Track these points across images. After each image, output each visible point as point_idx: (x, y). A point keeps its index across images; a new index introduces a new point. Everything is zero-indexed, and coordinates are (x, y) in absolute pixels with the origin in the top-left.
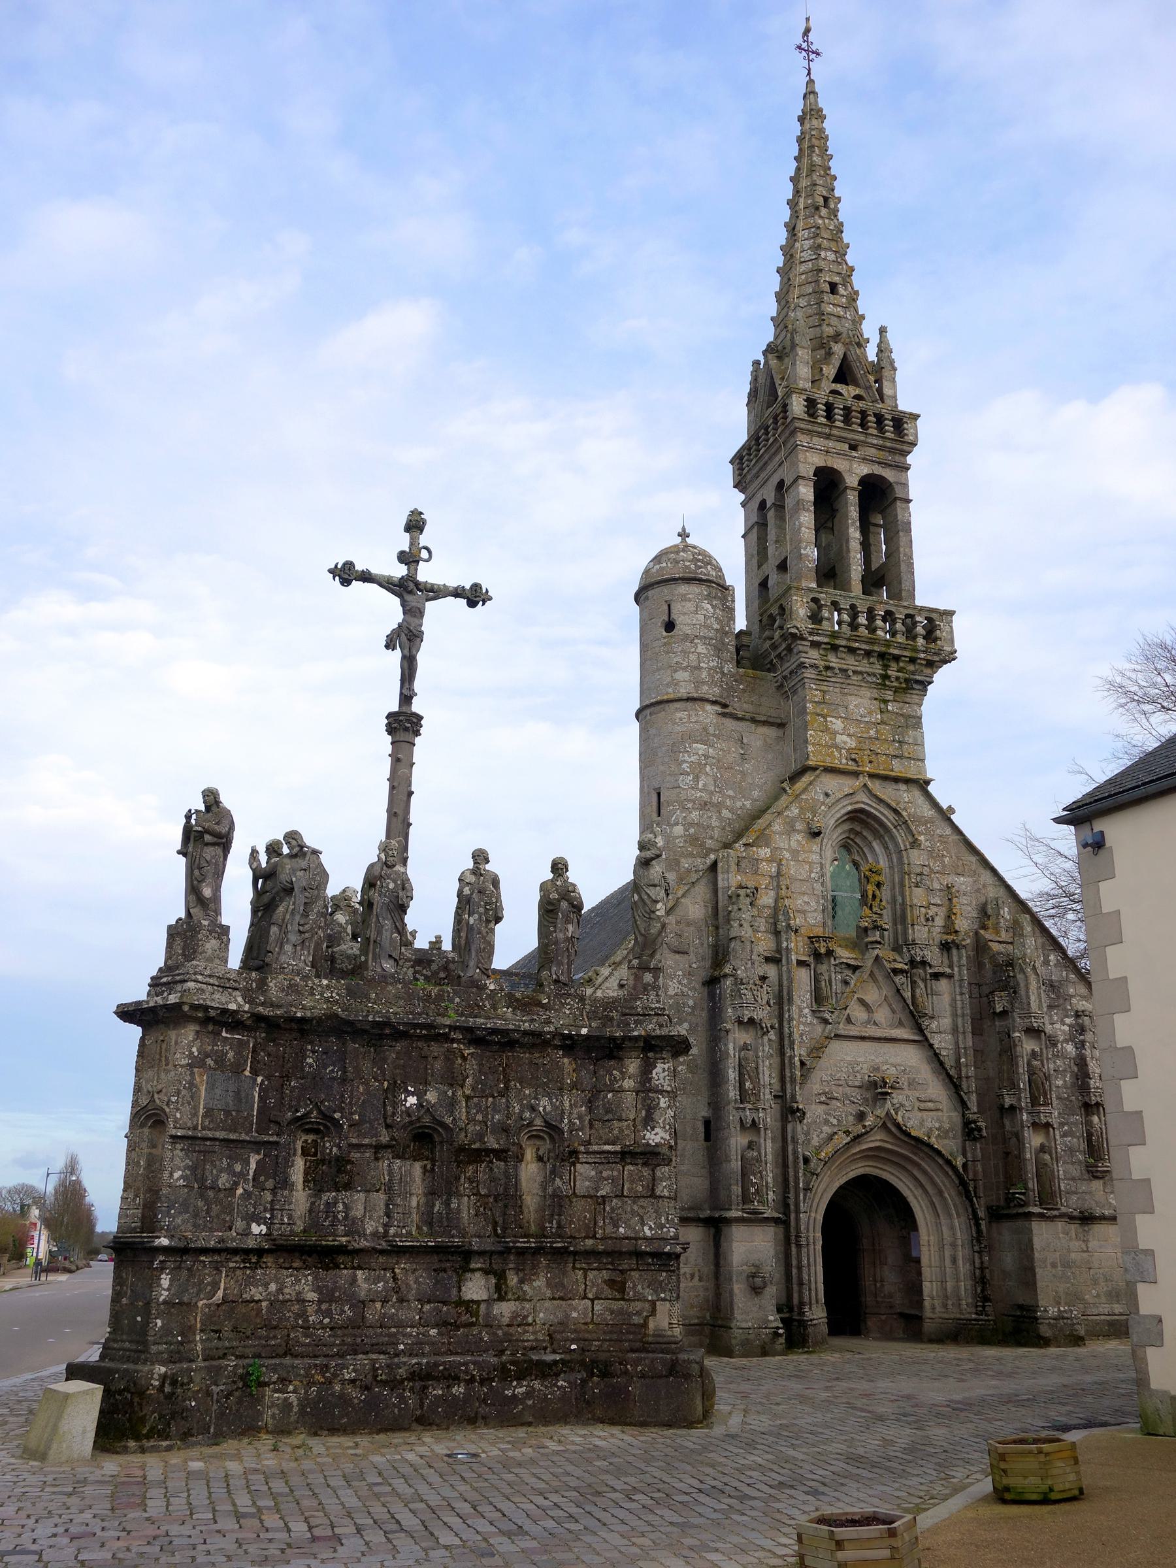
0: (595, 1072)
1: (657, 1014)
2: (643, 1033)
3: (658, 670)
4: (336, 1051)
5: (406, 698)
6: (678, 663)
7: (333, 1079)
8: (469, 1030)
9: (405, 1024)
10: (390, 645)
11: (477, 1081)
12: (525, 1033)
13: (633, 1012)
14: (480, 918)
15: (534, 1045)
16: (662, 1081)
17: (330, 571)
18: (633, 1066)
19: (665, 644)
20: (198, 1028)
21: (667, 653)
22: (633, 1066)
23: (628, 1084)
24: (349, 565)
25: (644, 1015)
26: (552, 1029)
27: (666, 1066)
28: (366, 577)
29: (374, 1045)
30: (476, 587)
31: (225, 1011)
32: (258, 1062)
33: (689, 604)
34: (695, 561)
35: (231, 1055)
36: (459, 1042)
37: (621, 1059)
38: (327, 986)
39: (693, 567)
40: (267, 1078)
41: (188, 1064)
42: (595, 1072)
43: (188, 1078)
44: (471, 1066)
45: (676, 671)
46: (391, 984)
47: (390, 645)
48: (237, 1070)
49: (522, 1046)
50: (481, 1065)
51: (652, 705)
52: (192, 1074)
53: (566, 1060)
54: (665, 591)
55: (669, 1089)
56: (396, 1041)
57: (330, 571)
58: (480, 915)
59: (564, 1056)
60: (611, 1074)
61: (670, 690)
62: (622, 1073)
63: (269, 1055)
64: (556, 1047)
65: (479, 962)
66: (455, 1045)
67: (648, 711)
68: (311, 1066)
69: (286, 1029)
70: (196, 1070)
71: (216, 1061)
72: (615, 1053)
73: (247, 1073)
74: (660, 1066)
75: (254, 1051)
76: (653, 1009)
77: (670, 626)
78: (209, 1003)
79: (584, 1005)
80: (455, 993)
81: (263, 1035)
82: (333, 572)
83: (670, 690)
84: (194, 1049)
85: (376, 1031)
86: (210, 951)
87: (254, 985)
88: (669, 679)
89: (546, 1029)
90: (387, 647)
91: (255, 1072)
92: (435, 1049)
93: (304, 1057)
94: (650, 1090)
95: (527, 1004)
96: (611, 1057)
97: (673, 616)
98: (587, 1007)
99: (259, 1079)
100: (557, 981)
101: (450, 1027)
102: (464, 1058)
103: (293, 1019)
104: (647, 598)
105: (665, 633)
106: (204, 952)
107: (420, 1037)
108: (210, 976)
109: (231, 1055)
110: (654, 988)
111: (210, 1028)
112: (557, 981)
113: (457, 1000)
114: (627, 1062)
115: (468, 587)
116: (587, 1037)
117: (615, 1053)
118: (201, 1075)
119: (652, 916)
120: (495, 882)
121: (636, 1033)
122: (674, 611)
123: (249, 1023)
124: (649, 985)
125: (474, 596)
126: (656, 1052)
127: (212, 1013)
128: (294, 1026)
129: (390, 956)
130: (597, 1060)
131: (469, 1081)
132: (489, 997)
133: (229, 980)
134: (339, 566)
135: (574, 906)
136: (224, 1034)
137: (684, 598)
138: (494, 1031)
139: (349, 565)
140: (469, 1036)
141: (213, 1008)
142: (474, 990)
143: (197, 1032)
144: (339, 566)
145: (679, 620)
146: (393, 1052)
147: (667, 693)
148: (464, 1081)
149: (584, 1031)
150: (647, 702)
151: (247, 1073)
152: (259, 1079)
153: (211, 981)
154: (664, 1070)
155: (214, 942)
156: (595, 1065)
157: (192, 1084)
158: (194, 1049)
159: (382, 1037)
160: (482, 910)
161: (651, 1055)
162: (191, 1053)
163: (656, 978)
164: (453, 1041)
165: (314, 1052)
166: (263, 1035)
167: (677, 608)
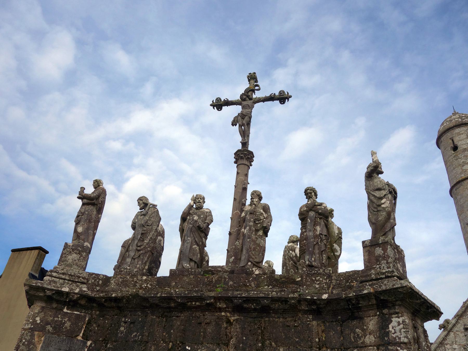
0: (342, 332)
1: (387, 277)
2: (372, 290)
3: (454, 169)
4: (141, 321)
5: (245, 144)
6: (463, 162)
7: (135, 341)
8: (228, 300)
9: (182, 298)
10: (234, 124)
11: (239, 341)
12: (274, 300)
13: (368, 278)
14: (250, 229)
15: (285, 311)
16: (398, 334)
17: (211, 105)
18: (372, 323)
19: (455, 156)
20: (43, 305)
21: (457, 159)
22: (372, 323)
23: (370, 339)
24: (218, 99)
25: (377, 279)
26: (296, 295)
27: (401, 320)
28: (228, 103)
29: (166, 316)
30: (282, 92)
31: (60, 293)
32: (91, 331)
33: (462, 136)
34: (460, 117)
35: (68, 324)
36: (225, 310)
37: (361, 318)
38: (145, 280)
39: (460, 120)
40: (94, 342)
41: (30, 328)
42: (342, 332)
43: (28, 338)
44: (235, 330)
45: (463, 166)
46: (186, 275)
47: (234, 124)
48: (72, 335)
49: (276, 311)
50: (243, 328)
51: (455, 185)
52: (32, 336)
53: (314, 323)
54: (449, 135)
55: (406, 340)
56: (181, 312)
57: (211, 105)
58: (250, 226)
59: (313, 320)
60: (354, 333)
61: (463, 175)
62: (363, 330)
63: (98, 326)
64: (306, 312)
65: (249, 257)
66: (223, 314)
67: (454, 189)
68: (122, 333)
69: (110, 308)
70: (36, 333)
71: (54, 328)
72: (356, 314)
73: (79, 338)
74: (395, 321)
75: (89, 323)
76: (383, 274)
77: (455, 148)
78: (45, 286)
79: (331, 280)
80: (230, 279)
81: (98, 313)
82: (213, 105)
83: (463, 175)
84: (38, 319)
85: (165, 305)
86: (70, 261)
87: (101, 282)
88: (460, 171)
89: (291, 295)
90: (233, 125)
91: (86, 338)
92: (209, 316)
93: (119, 326)
94: (389, 343)
95: (283, 283)
96: (353, 317)
97: (455, 143)
98: (334, 281)
99: (89, 343)
100: (310, 266)
101: (214, 298)
102: (228, 322)
103: (111, 299)
104: (441, 142)
105: (453, 152)
106: (65, 261)
107: (197, 308)
108: (63, 274)
109: (68, 324)
110: (384, 258)
111: (55, 305)
112: (310, 266)
113: (231, 283)
114: (367, 320)
115: (277, 94)
116: (328, 301)
117: (356, 314)
118: (39, 337)
119: (379, 209)
120: (266, 209)
121: (365, 292)
122: (455, 141)
123: (83, 302)
124: (380, 256)
125: (283, 98)
126: (389, 308)
127: (48, 293)
128: (113, 304)
129: (191, 260)
130: (343, 322)
131: (233, 341)
132: (254, 279)
133: (79, 277)
134: (214, 102)
135: (320, 214)
136: (65, 310)
137: (459, 134)
138: (248, 300)
139: (218, 99)
140: (231, 305)
141: (49, 289)
142: (244, 275)
143: (43, 308)
144: (214, 102)
145: (459, 144)
146: (178, 321)
147: (461, 177)
148: (229, 341)
149: (325, 296)
150: (452, 185)
151: (79, 338)
152: (89, 343)
153: (63, 277)
154: (399, 324)
155: (75, 255)
156: (341, 326)
157: (30, 342)
158: (38, 319)
159: (170, 309)
160: (252, 224)
161: (385, 311)
162: (35, 321)
163: (385, 250)
164: (220, 310)
165: (125, 322)
166: (98, 313)
167: (456, 139)
